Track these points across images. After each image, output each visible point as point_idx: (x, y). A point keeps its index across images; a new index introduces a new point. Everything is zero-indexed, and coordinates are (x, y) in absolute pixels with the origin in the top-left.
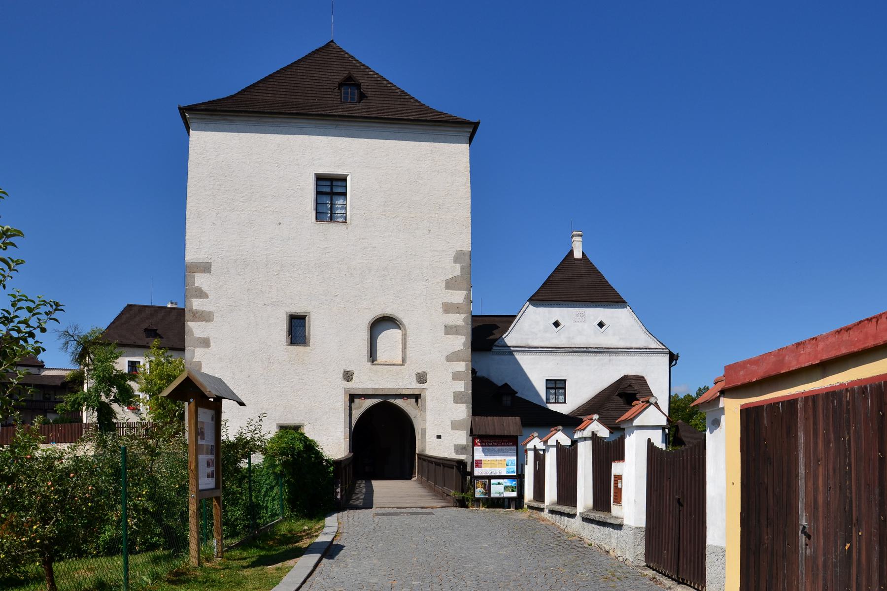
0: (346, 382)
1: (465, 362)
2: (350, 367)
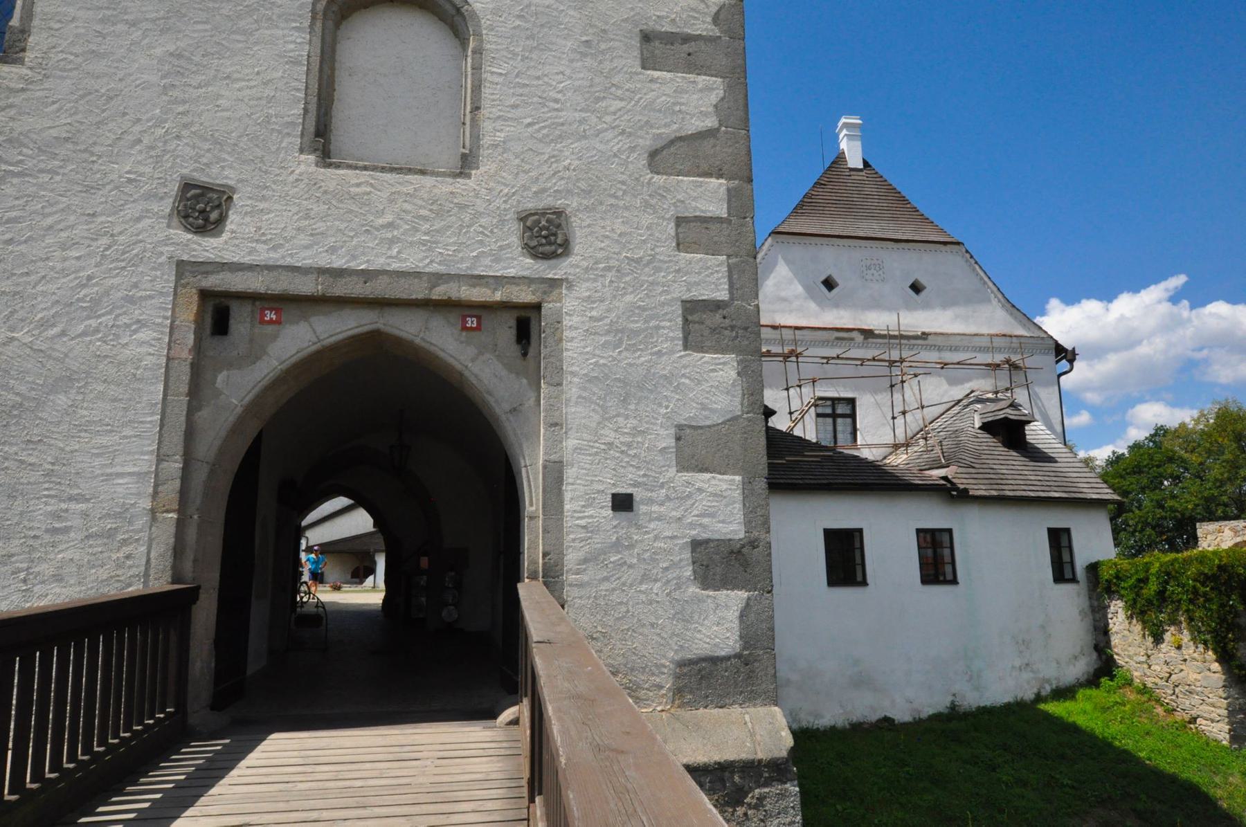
0: (190, 236)
1: (729, 179)
2: (215, 170)
